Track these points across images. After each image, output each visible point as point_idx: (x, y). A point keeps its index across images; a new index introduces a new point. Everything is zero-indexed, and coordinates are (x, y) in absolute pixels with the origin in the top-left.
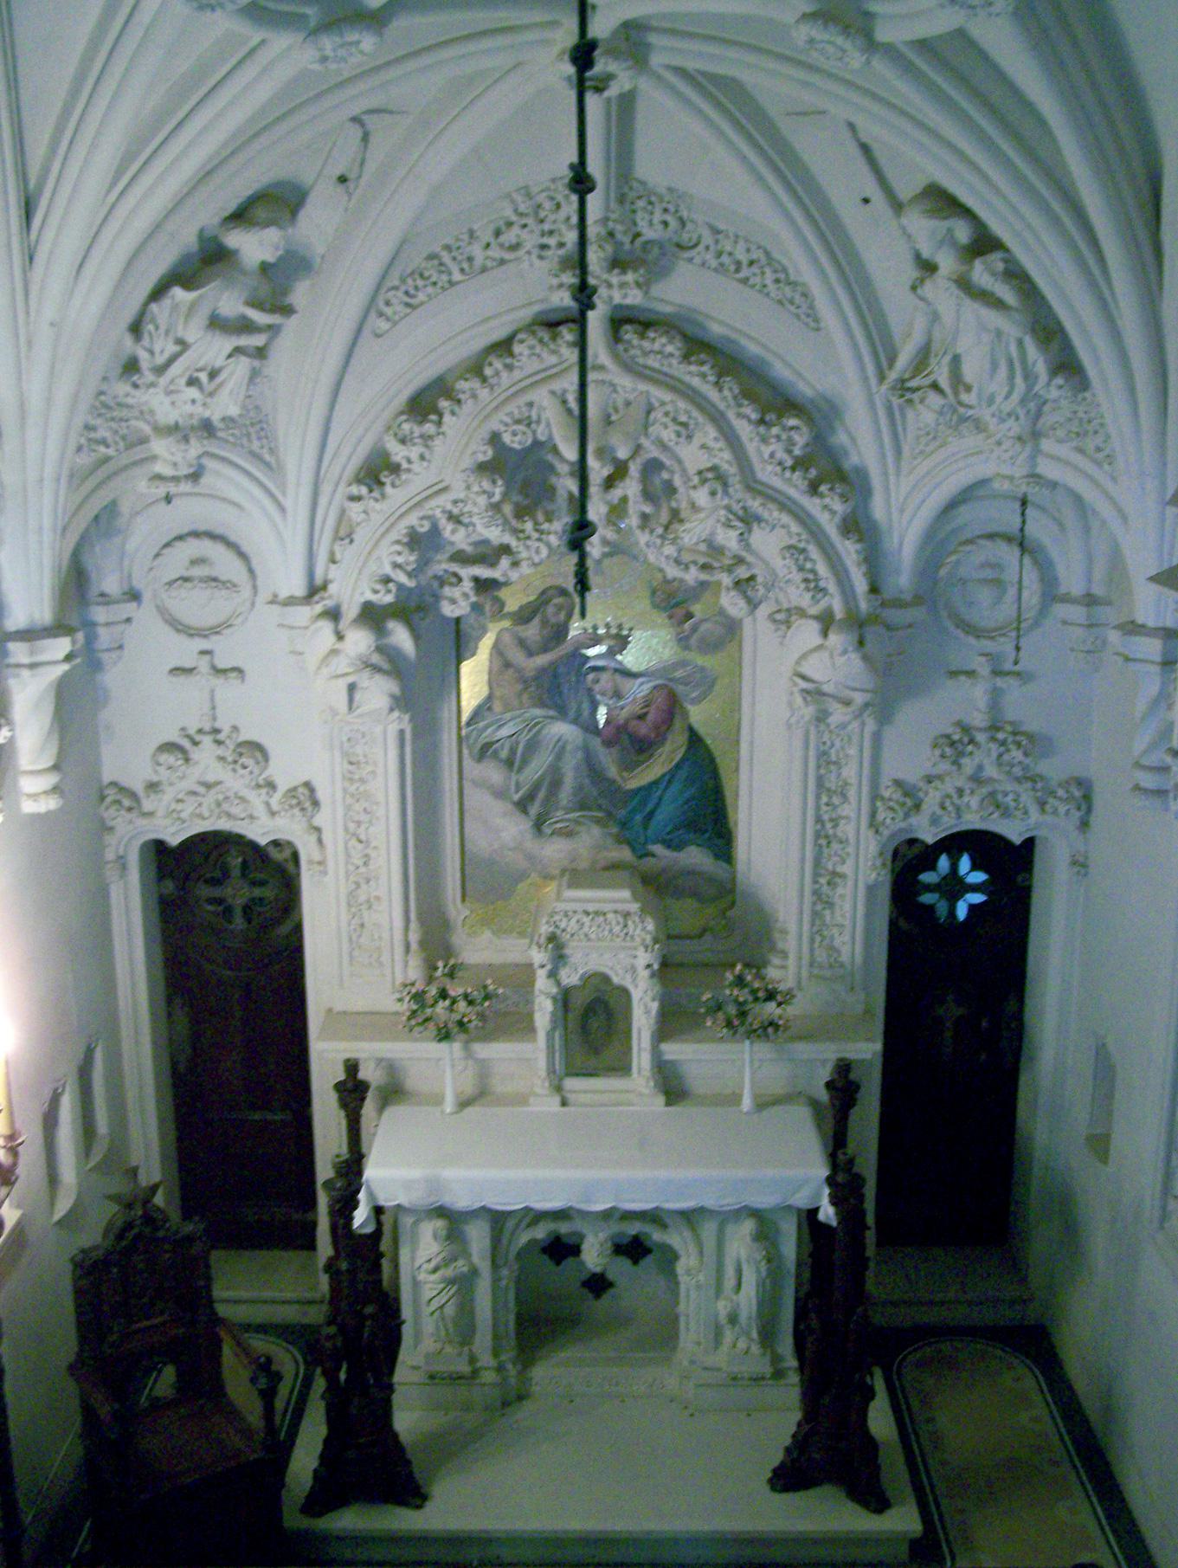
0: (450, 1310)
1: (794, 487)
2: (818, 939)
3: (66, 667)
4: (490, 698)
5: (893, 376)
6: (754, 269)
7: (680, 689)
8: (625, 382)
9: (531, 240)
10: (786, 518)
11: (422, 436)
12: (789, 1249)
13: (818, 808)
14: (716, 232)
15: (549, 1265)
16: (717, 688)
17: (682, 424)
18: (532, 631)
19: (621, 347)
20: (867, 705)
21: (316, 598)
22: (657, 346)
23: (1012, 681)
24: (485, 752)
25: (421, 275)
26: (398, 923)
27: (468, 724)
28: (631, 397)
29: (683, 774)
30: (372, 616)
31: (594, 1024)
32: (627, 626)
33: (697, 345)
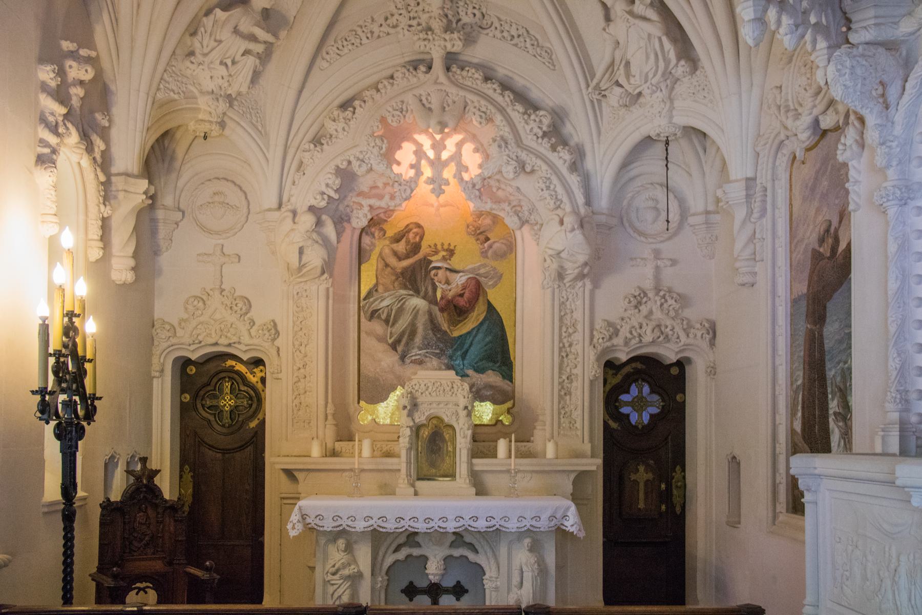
1: (543, 147)
4: (376, 285)
6: (522, 39)
7: (482, 280)
8: (453, 90)
9: (404, 21)
11: (344, 118)
13: (560, 335)
14: (500, 20)
18: (401, 247)
19: (450, 74)
22: (470, 74)
24: (374, 315)
27: (364, 299)
28: (456, 99)
29: (485, 327)
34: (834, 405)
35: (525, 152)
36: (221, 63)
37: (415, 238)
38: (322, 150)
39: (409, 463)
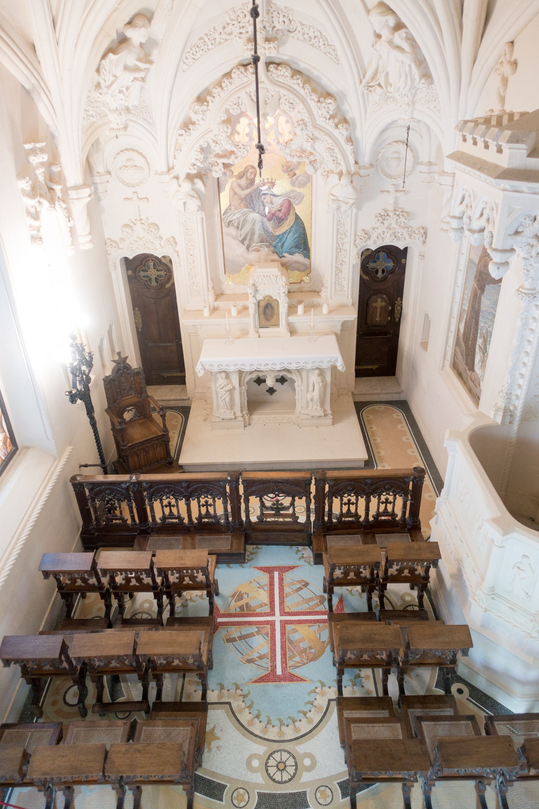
0: (227, 400)
1: (329, 125)
2: (337, 282)
3: (89, 199)
4: (230, 205)
5: (364, 81)
6: (316, 40)
7: (292, 201)
8: (272, 88)
9: (236, 31)
10: (327, 138)
11: (202, 111)
12: (328, 378)
13: (337, 239)
15: (256, 385)
16: (304, 199)
17: (291, 103)
19: (269, 74)
20: (354, 203)
21: (171, 172)
22: (282, 73)
23: (401, 193)
24: (229, 224)
25: (198, 46)
26: (205, 282)
27: (224, 215)
29: (293, 229)
30: (190, 177)
31: (267, 311)
32: (274, 179)
33: (297, 72)
34: (480, 341)
35: (318, 131)
36: (120, 92)
37: (251, 175)
38: (190, 134)
39: (255, 321)
